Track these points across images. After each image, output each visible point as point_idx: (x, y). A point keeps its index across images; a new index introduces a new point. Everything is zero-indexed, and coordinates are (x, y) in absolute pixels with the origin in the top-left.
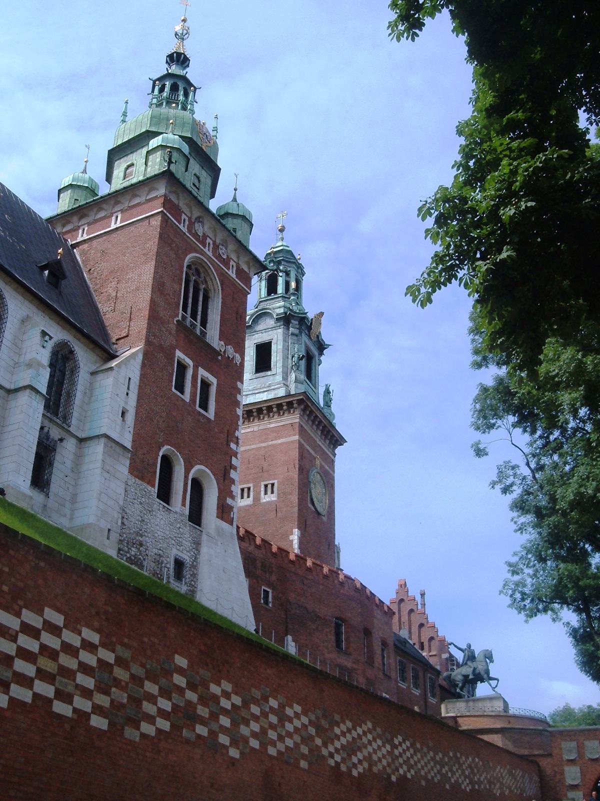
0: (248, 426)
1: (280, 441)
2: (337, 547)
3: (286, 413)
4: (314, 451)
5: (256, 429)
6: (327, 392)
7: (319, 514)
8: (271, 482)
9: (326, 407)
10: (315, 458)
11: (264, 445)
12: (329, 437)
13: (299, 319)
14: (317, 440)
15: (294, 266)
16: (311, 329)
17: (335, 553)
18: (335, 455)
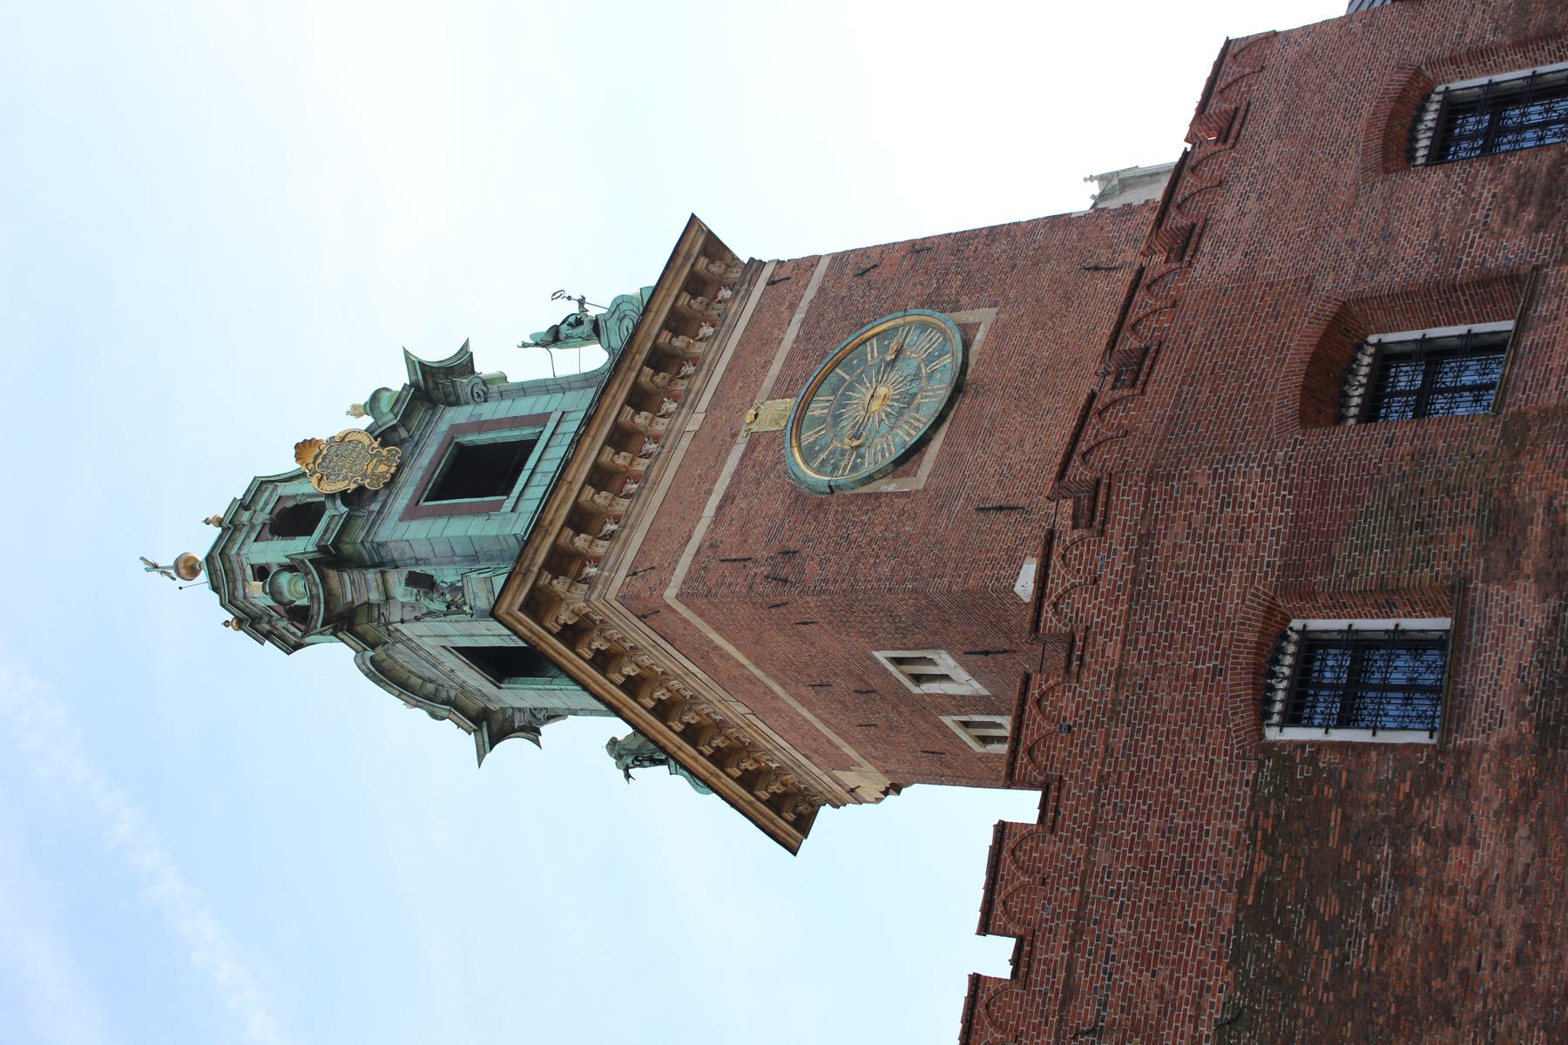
0: (748, 729)
1: (729, 648)
2: (1103, 196)
3: (614, 633)
4: (728, 451)
5: (741, 709)
6: (554, 338)
7: (958, 389)
8: (891, 668)
9: (604, 338)
10: (754, 441)
11: (777, 688)
12: (679, 342)
13: (333, 574)
14: (695, 423)
15: (234, 551)
16: (361, 489)
17: (1128, 210)
18: (756, 266)
